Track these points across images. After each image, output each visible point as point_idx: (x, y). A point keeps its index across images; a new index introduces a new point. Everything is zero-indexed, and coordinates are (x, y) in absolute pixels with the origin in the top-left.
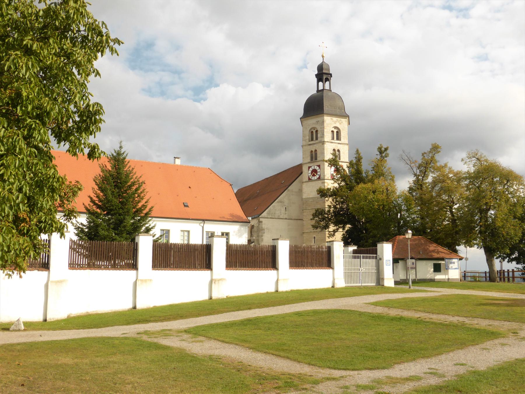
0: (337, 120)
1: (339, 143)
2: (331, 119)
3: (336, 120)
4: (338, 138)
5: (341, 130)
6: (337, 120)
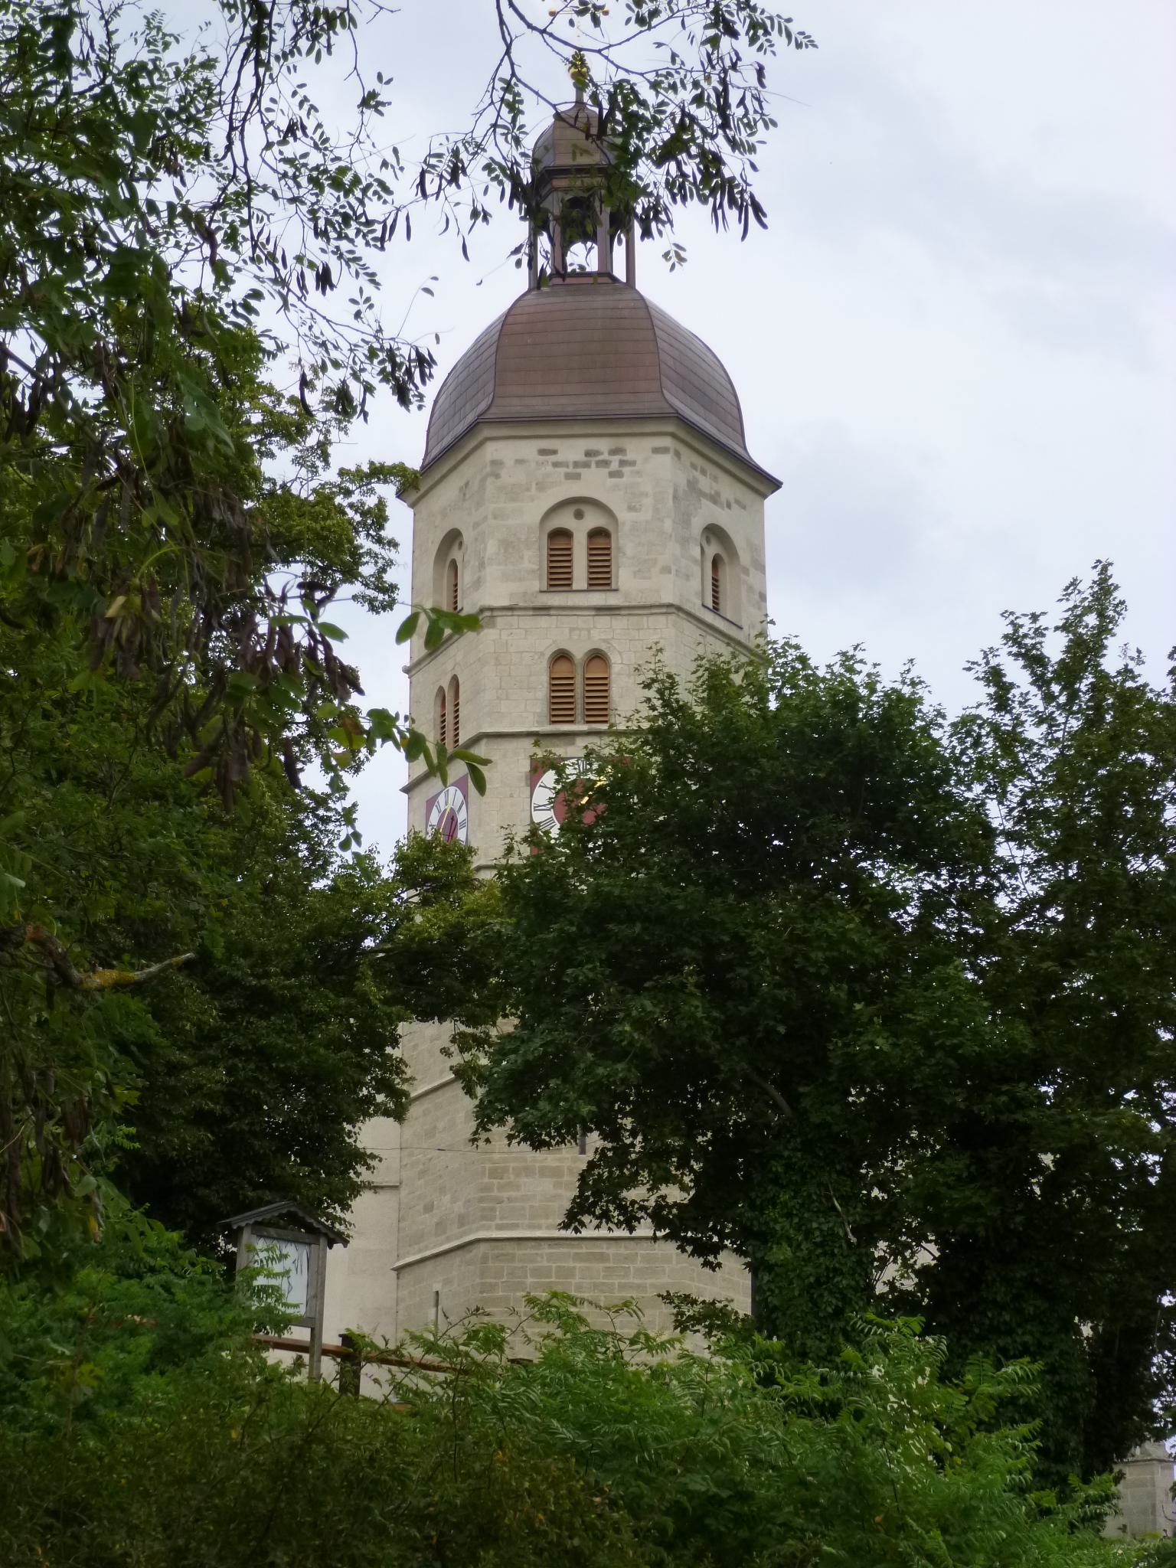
0: (588, 454)
1: (601, 610)
2: (543, 452)
3: (580, 457)
4: (601, 577)
5: (623, 515)
6: (588, 454)
